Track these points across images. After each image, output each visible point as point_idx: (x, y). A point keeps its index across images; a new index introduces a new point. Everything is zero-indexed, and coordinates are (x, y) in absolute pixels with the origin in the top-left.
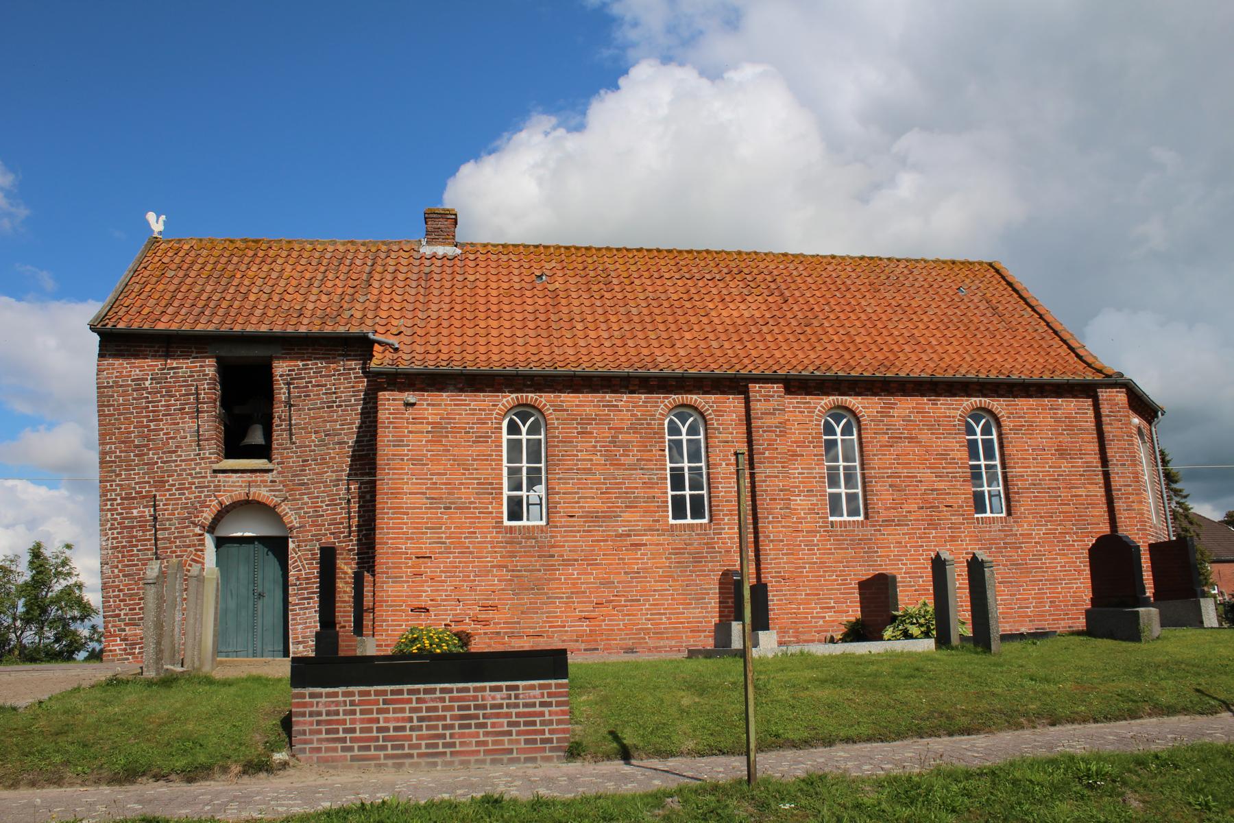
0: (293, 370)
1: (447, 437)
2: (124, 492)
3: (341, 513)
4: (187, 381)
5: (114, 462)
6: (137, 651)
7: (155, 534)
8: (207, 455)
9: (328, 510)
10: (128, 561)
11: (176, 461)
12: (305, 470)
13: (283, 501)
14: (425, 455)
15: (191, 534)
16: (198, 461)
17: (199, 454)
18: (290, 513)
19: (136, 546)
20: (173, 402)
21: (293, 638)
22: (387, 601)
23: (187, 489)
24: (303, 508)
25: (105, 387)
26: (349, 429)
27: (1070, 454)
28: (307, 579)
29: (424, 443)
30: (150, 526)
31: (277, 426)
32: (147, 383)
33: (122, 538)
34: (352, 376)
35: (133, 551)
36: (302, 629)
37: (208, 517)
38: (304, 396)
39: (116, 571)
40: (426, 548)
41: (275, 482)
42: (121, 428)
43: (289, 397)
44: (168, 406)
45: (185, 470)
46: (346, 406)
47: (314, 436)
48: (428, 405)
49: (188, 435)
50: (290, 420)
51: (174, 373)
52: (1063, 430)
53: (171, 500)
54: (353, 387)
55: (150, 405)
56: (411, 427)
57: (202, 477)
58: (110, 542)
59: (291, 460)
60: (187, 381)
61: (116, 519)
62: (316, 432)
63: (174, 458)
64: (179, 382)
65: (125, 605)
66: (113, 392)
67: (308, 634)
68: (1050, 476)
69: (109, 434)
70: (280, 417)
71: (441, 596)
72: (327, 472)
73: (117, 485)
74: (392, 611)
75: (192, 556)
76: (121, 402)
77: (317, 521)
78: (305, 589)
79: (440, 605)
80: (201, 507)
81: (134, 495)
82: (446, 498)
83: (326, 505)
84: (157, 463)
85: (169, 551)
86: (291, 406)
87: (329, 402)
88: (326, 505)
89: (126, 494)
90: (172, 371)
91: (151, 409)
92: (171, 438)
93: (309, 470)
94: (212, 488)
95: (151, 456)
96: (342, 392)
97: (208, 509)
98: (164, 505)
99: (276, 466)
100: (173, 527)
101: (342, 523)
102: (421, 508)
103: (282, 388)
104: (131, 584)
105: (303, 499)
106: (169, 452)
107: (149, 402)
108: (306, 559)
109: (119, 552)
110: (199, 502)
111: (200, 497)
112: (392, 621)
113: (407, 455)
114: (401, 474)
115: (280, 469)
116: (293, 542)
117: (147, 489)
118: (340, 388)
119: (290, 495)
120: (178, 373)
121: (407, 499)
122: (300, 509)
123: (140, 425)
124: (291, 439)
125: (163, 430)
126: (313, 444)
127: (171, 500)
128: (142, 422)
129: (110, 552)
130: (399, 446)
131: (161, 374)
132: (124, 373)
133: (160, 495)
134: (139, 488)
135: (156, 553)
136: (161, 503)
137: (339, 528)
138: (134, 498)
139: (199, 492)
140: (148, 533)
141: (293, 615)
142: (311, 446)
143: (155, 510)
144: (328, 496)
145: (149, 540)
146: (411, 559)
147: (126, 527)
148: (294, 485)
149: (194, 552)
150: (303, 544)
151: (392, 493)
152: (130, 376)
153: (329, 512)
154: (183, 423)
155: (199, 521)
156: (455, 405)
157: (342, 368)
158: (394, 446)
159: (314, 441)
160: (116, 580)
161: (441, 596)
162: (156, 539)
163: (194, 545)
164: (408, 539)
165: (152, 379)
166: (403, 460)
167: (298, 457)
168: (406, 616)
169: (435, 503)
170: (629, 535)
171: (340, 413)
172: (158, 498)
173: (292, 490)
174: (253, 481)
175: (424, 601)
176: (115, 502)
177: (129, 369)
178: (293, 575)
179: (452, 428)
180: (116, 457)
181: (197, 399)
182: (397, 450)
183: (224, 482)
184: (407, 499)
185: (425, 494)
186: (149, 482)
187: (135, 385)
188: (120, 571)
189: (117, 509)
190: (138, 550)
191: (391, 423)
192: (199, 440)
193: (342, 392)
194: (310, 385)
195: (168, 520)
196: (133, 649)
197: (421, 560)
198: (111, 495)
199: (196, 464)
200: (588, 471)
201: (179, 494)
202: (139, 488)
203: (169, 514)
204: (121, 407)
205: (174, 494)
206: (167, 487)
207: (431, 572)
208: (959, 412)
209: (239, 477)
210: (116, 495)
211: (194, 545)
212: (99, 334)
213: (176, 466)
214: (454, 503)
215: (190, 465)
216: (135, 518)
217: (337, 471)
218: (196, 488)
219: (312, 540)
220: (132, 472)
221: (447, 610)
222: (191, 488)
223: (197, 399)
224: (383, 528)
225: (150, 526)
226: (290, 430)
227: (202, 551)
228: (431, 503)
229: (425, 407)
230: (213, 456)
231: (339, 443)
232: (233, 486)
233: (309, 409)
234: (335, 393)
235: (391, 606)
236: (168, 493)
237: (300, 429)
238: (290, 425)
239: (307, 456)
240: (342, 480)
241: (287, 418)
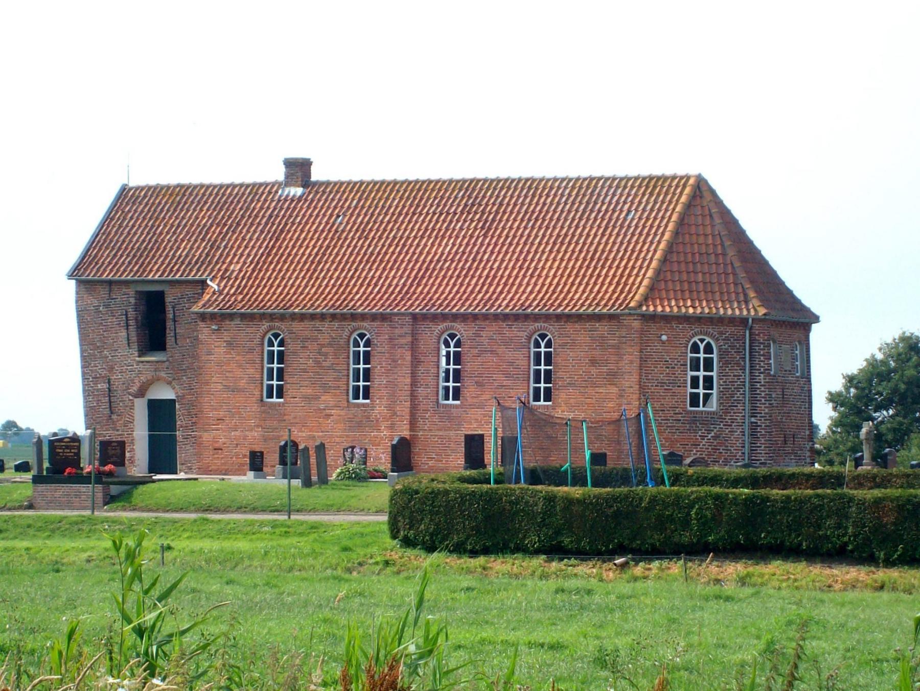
7: (110, 399)
32: (101, 308)
43: (174, 316)
50: (175, 330)
56: (217, 344)
162: (110, 402)
170: (324, 409)
200: (305, 371)
208: (526, 333)
227: (133, 409)
238: (175, 333)
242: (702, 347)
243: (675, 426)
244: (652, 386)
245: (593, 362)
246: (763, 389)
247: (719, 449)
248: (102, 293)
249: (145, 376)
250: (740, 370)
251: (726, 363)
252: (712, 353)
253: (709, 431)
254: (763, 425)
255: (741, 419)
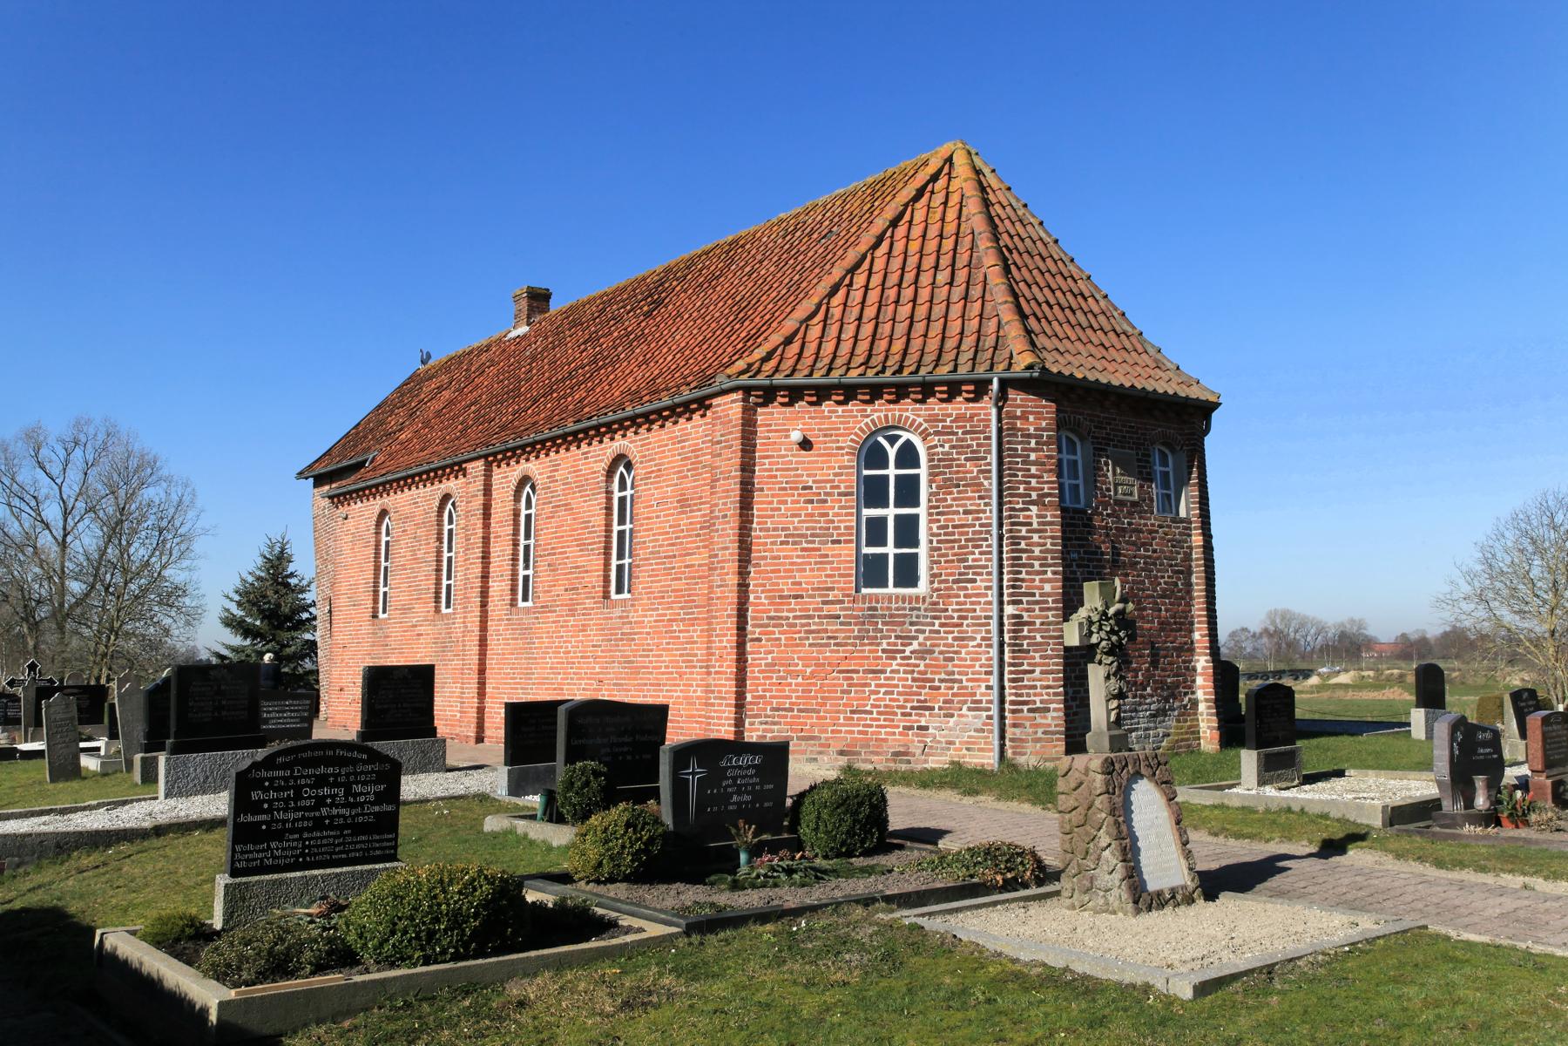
27: (689, 506)
52: (688, 470)
68: (667, 539)
242: (892, 453)
243: (826, 631)
244: (772, 543)
245: (684, 503)
246: (1036, 538)
247: (933, 680)
250: (980, 498)
251: (947, 485)
252: (917, 466)
253: (907, 639)
254: (1038, 621)
255: (983, 610)
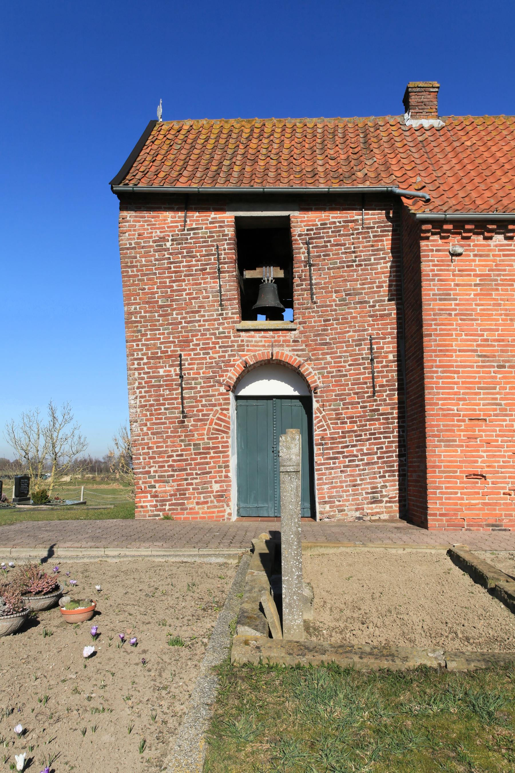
0: (312, 230)
1: (497, 290)
2: (149, 352)
3: (364, 373)
4: (207, 242)
5: (140, 322)
6: (167, 507)
8: (230, 315)
9: (351, 370)
10: (157, 419)
11: (200, 321)
12: (327, 330)
13: (306, 361)
14: (474, 310)
15: (217, 393)
16: (221, 321)
17: (221, 314)
18: (314, 372)
19: (164, 404)
20: (194, 263)
21: (320, 498)
22: (440, 467)
23: (211, 348)
24: (326, 368)
25: (128, 249)
26: (370, 288)
28: (333, 438)
29: (472, 296)
30: (176, 385)
31: (297, 286)
32: (169, 244)
33: (150, 396)
34: (371, 235)
35: (160, 409)
36: (328, 489)
37: (233, 376)
38: (324, 256)
39: (145, 429)
40: (480, 410)
41: (298, 341)
42: (144, 289)
44: (189, 266)
45: (208, 330)
46: (366, 265)
47: (334, 295)
48: (475, 255)
49: (210, 295)
50: (311, 279)
51: (194, 234)
53: (196, 359)
54: (372, 246)
55: (172, 266)
56: (458, 280)
57: (226, 337)
58: (138, 400)
59: (313, 320)
60: (207, 242)
61: (143, 378)
62: (336, 292)
63: (197, 318)
64: (199, 242)
65: (154, 462)
66: (136, 253)
67: (335, 494)
69: (133, 295)
70: (300, 277)
71: (499, 462)
72: (349, 332)
73: (143, 345)
74: (446, 477)
75: (218, 415)
76: (144, 263)
77: (340, 381)
78: (331, 448)
79: (498, 472)
80: (226, 366)
81: (159, 355)
82: (499, 356)
83: (349, 365)
84: (181, 323)
85: (195, 409)
86: (311, 265)
87: (348, 262)
88: (349, 365)
89: (152, 353)
90: (192, 232)
91: (173, 269)
92: (194, 298)
93: (331, 329)
94: (236, 348)
95: (175, 316)
96: (362, 251)
97: (232, 368)
98: (189, 364)
99: (298, 326)
100: (199, 386)
101: (366, 383)
102: (472, 367)
103: (301, 248)
104: (159, 442)
105: (326, 359)
106: (193, 312)
107: (171, 263)
108: (330, 419)
109: (147, 410)
110: (223, 362)
111: (224, 356)
112: (447, 488)
113: (455, 310)
114: (450, 330)
115: (302, 329)
116: (317, 401)
117: (172, 349)
118: (359, 247)
119: (313, 355)
120: (198, 233)
121: (457, 356)
122: (323, 368)
123: (163, 285)
124: (312, 298)
125: (185, 290)
126: (334, 303)
127: (196, 359)
128: (165, 282)
129: (139, 410)
130: (445, 300)
131: (182, 235)
132: (146, 235)
133: (185, 355)
134: (165, 347)
135: (183, 412)
136: (186, 363)
137: (363, 388)
138: (160, 358)
139: (223, 352)
140: (174, 392)
141: (319, 475)
142: (332, 306)
143: (181, 369)
144: (351, 356)
145: (176, 399)
146: (464, 421)
147: (153, 386)
148: (316, 344)
149: (220, 411)
150: (328, 404)
151: (441, 351)
152: (151, 237)
153: (352, 372)
154: (204, 283)
155: (224, 380)
156: (504, 255)
157: (360, 227)
158: (440, 300)
159: (334, 301)
160: (146, 437)
161: (499, 462)
162: (183, 398)
163: (220, 404)
164: (460, 399)
165: (172, 240)
166: (450, 315)
167: (319, 317)
168: (461, 483)
169: (488, 361)
171: (360, 272)
172: (183, 357)
173: (314, 350)
174: (275, 341)
175: (480, 466)
176: (142, 362)
177: (150, 231)
178: (319, 435)
179: (502, 280)
180: (141, 317)
181: (219, 259)
182: (444, 305)
183: (247, 341)
184: (457, 356)
185: (476, 351)
186: (174, 342)
187: (157, 246)
188: (149, 429)
189: (143, 369)
190: (166, 409)
191: (436, 275)
192: (221, 300)
193: (362, 251)
194: (328, 244)
195: (194, 379)
196: (162, 505)
197: (476, 422)
198: (138, 355)
199: (219, 324)
201: (204, 354)
202: (165, 347)
203: (194, 374)
204: (144, 268)
205: (199, 354)
206: (191, 347)
207: (486, 436)
209: (262, 337)
210: (142, 355)
211: (220, 404)
212: (119, 197)
213: (199, 326)
214: (508, 361)
215: (213, 325)
216: (162, 377)
217: (359, 331)
218: (220, 347)
219: (336, 400)
220: (157, 332)
221: (505, 478)
222: (215, 348)
223: (219, 259)
224: (432, 388)
225: (176, 385)
226: (311, 289)
227: (227, 409)
228: (483, 362)
229: (472, 258)
230: (235, 316)
231: (361, 303)
232: (256, 346)
233: (329, 269)
234: (354, 252)
235: (444, 472)
236: (192, 353)
237: (320, 288)
238: (311, 284)
239: (328, 315)
240: (364, 340)
241: (308, 277)
248: (169, 220)
249: (252, 354)
